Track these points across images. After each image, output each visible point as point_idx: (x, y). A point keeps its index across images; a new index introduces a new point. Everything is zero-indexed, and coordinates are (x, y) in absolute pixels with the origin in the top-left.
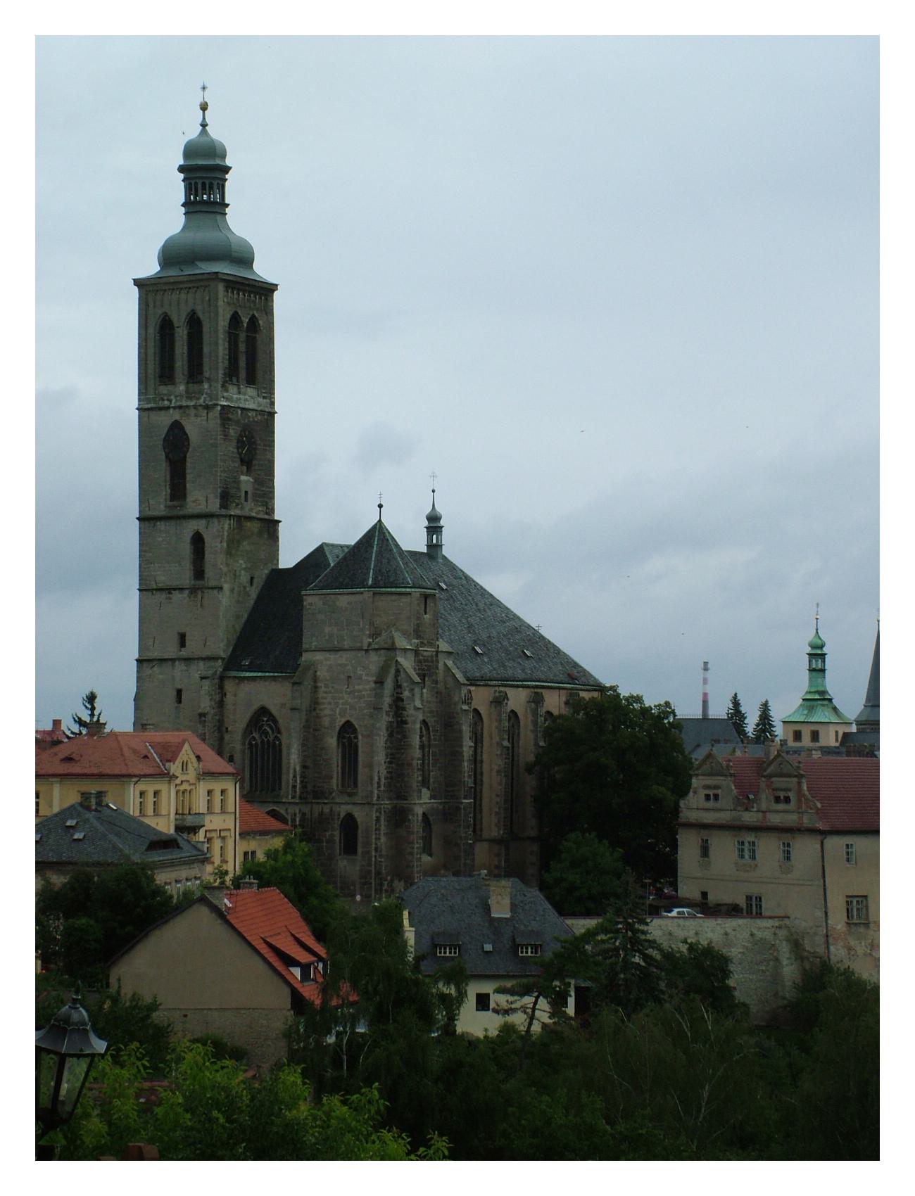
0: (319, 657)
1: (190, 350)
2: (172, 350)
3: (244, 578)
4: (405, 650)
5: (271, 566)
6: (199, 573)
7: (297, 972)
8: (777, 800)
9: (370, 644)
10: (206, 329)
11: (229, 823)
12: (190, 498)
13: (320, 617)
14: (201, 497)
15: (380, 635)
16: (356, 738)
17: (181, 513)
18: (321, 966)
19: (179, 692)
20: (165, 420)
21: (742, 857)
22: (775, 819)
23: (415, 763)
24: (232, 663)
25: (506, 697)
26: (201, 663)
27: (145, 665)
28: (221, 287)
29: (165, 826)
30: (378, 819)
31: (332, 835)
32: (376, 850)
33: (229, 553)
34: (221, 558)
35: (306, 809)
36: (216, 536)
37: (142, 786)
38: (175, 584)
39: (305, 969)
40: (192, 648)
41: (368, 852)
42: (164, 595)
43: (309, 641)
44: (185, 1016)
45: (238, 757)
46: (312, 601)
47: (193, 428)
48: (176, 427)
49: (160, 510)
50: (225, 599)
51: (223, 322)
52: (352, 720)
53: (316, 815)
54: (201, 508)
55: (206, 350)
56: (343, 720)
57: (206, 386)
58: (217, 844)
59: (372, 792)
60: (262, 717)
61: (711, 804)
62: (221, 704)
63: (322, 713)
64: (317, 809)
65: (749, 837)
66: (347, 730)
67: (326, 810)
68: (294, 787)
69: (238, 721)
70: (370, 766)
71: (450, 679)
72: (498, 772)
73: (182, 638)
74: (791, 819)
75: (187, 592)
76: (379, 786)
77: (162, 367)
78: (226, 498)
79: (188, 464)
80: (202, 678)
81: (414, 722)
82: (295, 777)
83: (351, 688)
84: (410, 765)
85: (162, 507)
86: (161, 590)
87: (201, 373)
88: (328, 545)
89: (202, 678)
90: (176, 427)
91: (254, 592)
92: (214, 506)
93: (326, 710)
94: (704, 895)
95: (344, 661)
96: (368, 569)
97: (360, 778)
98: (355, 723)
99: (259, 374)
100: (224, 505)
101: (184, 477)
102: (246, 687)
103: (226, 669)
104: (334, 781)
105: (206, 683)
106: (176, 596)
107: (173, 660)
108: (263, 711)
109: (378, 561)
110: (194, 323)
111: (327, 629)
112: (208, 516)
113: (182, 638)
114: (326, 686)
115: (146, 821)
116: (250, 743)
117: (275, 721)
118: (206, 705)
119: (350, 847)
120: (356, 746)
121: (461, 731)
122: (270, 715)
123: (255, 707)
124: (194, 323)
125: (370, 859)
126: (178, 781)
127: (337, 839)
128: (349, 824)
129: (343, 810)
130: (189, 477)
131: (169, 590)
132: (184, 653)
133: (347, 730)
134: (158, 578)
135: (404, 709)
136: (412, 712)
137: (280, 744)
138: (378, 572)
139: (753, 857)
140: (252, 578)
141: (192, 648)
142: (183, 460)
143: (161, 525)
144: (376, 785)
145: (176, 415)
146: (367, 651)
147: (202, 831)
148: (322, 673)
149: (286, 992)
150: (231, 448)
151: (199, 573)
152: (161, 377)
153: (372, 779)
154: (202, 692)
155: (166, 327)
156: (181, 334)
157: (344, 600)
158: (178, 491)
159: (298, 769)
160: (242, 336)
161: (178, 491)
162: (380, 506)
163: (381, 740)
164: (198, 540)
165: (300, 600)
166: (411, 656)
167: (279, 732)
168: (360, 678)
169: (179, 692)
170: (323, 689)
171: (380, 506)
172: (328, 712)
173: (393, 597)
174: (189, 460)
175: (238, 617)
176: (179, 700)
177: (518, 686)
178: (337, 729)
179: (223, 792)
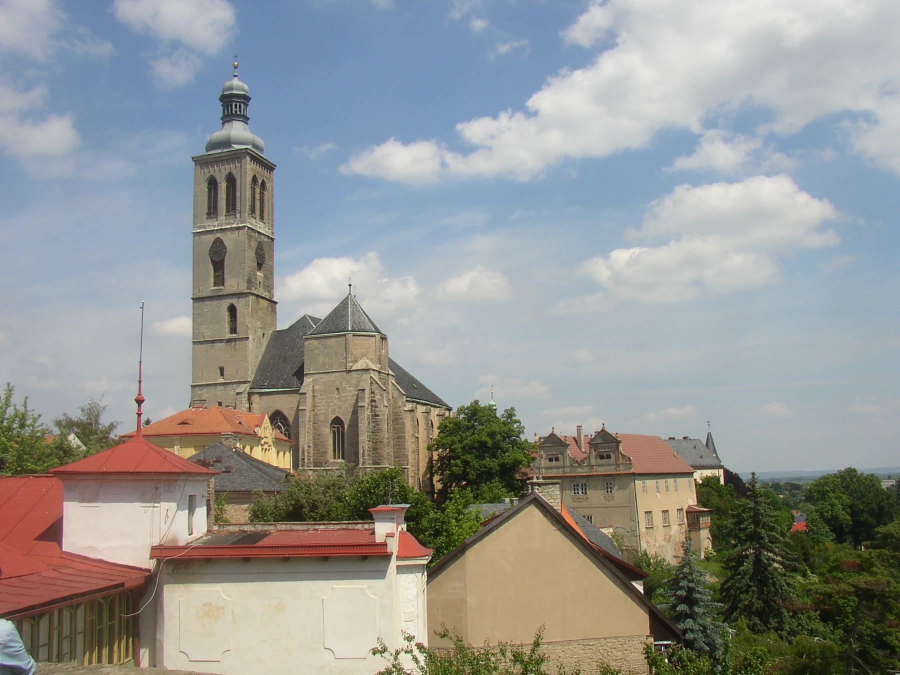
1: (228, 195)
2: (216, 196)
3: (260, 334)
6: (233, 330)
8: (602, 457)
10: (238, 183)
13: (316, 352)
14: (233, 283)
15: (357, 361)
20: (211, 238)
22: (601, 471)
23: (385, 441)
24: (257, 384)
28: (248, 158)
36: (244, 307)
40: (229, 376)
47: (229, 240)
48: (219, 241)
49: (210, 288)
50: (251, 344)
51: (249, 179)
55: (238, 194)
56: (334, 416)
57: (238, 216)
61: (554, 463)
68: (303, 459)
71: (396, 392)
73: (222, 370)
74: (611, 470)
77: (209, 208)
78: (249, 281)
81: (384, 415)
82: (303, 452)
87: (234, 209)
90: (219, 241)
96: (347, 322)
99: (266, 216)
102: (265, 398)
110: (231, 180)
112: (240, 295)
113: (222, 370)
121: (403, 424)
124: (231, 180)
126: (262, 442)
131: (213, 342)
132: (221, 380)
136: (382, 408)
138: (354, 322)
141: (229, 376)
145: (218, 235)
150: (253, 254)
151: (233, 330)
152: (209, 214)
155: (212, 183)
156: (223, 186)
158: (220, 280)
159: (306, 447)
160: (258, 190)
161: (220, 280)
164: (232, 310)
171: (350, 285)
172: (323, 412)
175: (257, 357)
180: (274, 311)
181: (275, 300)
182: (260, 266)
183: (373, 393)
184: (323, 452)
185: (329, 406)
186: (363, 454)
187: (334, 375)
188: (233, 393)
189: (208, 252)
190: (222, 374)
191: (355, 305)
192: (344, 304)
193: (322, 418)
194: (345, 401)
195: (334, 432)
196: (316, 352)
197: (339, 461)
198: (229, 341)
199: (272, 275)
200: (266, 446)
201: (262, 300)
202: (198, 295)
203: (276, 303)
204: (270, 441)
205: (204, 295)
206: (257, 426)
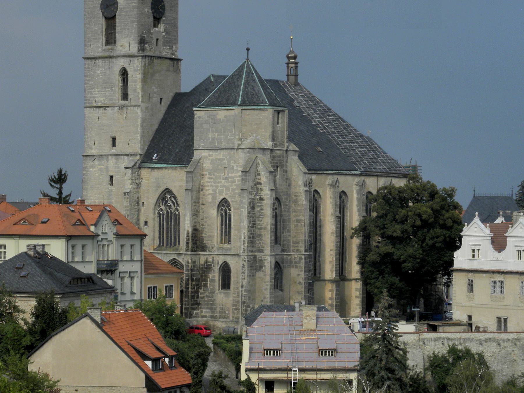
0: (205, 153)
4: (264, 149)
5: (175, 91)
6: (125, 96)
7: (149, 363)
9: (239, 145)
11: (137, 267)
12: (118, 44)
13: (205, 126)
14: (127, 42)
16: (230, 210)
17: (112, 54)
18: (167, 360)
19: (112, 177)
21: (495, 291)
24: (146, 158)
25: (337, 181)
26: (126, 158)
27: (88, 158)
29: (90, 269)
30: (243, 266)
31: (214, 277)
32: (242, 286)
33: (144, 81)
34: (139, 86)
35: (196, 258)
37: (72, 242)
38: (108, 102)
39: (155, 361)
40: (120, 147)
41: (238, 288)
42: (101, 111)
43: (197, 143)
44: (76, 390)
45: (150, 223)
46: (200, 114)
52: (227, 198)
53: (202, 262)
54: (126, 50)
56: (221, 198)
58: (127, 280)
59: (240, 247)
60: (166, 196)
62: (139, 185)
63: (207, 193)
64: (203, 260)
65: (498, 278)
66: (224, 204)
67: (210, 259)
69: (150, 198)
70: (239, 230)
72: (332, 233)
73: (114, 139)
75: (116, 108)
76: (244, 243)
78: (142, 42)
79: (117, 20)
80: (126, 168)
82: (188, 236)
83: (226, 175)
84: (265, 228)
85: (100, 49)
86: (99, 107)
88: (214, 76)
89: (126, 168)
91: (163, 109)
92: (134, 49)
93: (209, 191)
94: (470, 317)
95: (221, 157)
97: (232, 236)
98: (229, 200)
100: (142, 49)
101: (114, 28)
102: (156, 173)
103: (143, 162)
104: (215, 239)
105: (129, 171)
106: (109, 109)
107: (107, 155)
108: (167, 191)
109: (245, 87)
111: (210, 135)
114: (210, 174)
115: (73, 265)
116: (159, 213)
117: (175, 198)
118: (128, 187)
119: (226, 284)
120: (230, 215)
122: (173, 194)
123: (162, 189)
125: (238, 293)
126: (100, 238)
127: (217, 278)
128: (225, 270)
129: (221, 260)
130: (118, 29)
131: (105, 107)
133: (224, 204)
134: (97, 99)
135: (261, 190)
137: (179, 214)
138: (245, 94)
139: (502, 292)
140: (161, 99)
142: (114, 17)
143: (100, 62)
144: (242, 242)
147: (117, 273)
148: (207, 165)
149: (143, 375)
150: (148, 10)
151: (125, 96)
153: (240, 238)
154: (126, 178)
157: (222, 113)
158: (111, 39)
162: (248, 49)
163: (245, 213)
164: (124, 73)
165: (192, 114)
166: (268, 154)
167: (178, 205)
168: (233, 169)
169: (112, 177)
170: (207, 176)
171: (248, 49)
172: (210, 192)
173: (255, 112)
174: (117, 17)
176: (112, 184)
177: (346, 174)
178: (217, 203)
179: (132, 246)
180: (177, 71)
181: (179, 55)
182: (157, 20)
183: (259, 175)
184: (210, 236)
185: (217, 187)
186: (244, 241)
187: (223, 152)
188: (123, 165)
189: (98, 6)
190: (114, 145)
191: (249, 73)
192: (240, 71)
193: (210, 198)
195: (222, 215)
196: (205, 126)
197: (225, 246)
198: (121, 107)
199: (177, 28)
200: (105, 242)
201: (156, 61)
202: (92, 54)
203: (181, 60)
204: (111, 236)
205: (97, 54)
206: (92, 225)
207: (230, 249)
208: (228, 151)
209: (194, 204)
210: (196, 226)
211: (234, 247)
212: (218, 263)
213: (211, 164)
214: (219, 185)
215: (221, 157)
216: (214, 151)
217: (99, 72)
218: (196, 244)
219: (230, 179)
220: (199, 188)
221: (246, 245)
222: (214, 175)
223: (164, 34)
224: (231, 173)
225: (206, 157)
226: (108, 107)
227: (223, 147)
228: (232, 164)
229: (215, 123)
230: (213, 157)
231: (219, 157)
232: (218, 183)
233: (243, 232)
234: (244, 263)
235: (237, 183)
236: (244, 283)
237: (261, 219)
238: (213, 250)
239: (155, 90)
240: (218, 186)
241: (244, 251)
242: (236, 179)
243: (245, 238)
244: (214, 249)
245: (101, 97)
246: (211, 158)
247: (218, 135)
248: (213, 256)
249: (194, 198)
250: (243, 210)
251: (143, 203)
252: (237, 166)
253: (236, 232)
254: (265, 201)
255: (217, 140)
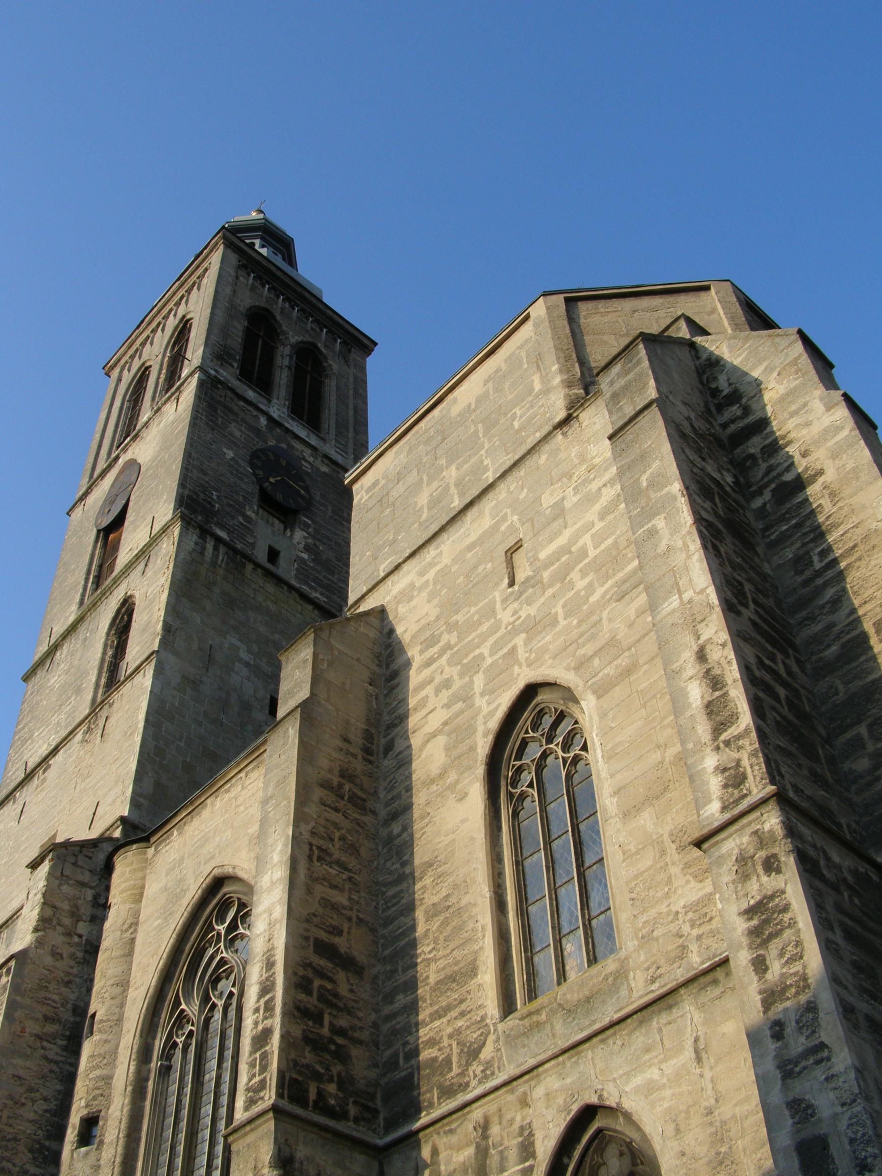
144: (703, 729)
146: (566, 421)
178: (483, 746)
194: (562, 576)
207: (621, 975)
208: (521, 472)
209: (318, 793)
210: (337, 931)
211: (646, 939)
212: (527, 1150)
213: (431, 596)
214: (485, 650)
215: (487, 522)
216: (445, 536)
217: (52, 681)
218: (341, 1056)
219: (546, 575)
220: (369, 737)
221: (746, 719)
222: (451, 627)
223: (305, 556)
224: (551, 541)
225: (407, 595)
226: (54, 752)
227: (491, 480)
228: (548, 500)
229: (444, 439)
230: (446, 560)
231: (473, 538)
232: (478, 647)
233: (688, 656)
234: (761, 884)
235: (592, 553)
236: (825, 1103)
237: (829, 593)
238: (476, 1068)
239: (244, 655)
240: (481, 657)
241: (735, 779)
242: (587, 539)
243: (715, 682)
244: (486, 1053)
245: (44, 742)
246: (431, 575)
247: (457, 469)
248: (477, 1113)
249: (324, 762)
250: (659, 522)
251: (94, 1016)
252: (576, 490)
253: (646, 819)
254: (830, 476)
255: (457, 485)
